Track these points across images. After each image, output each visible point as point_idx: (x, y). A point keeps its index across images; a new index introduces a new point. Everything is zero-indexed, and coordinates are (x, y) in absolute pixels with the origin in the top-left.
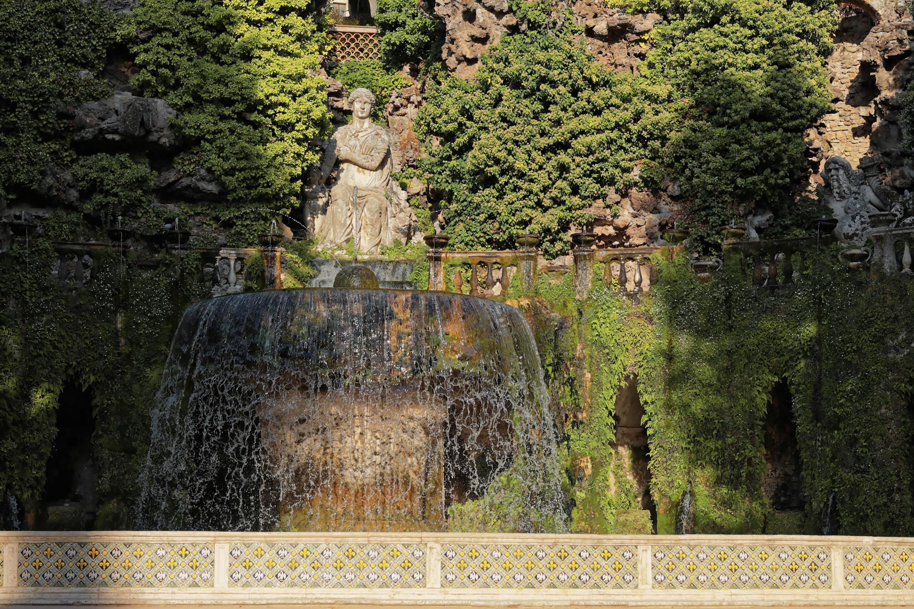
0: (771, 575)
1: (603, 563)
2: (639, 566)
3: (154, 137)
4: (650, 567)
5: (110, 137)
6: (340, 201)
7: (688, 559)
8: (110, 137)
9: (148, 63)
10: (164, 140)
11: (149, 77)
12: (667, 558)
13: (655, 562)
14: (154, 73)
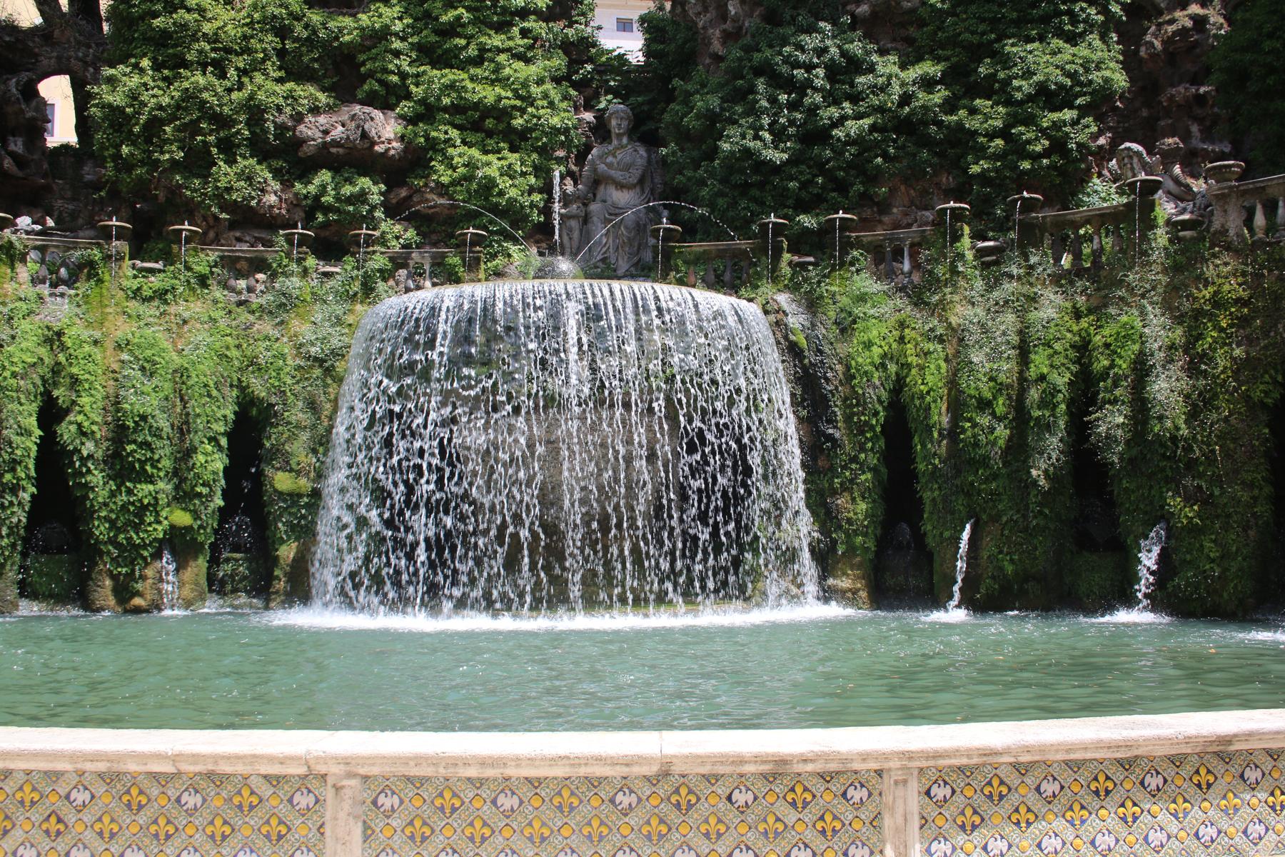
0: (1224, 825)
1: (791, 816)
2: (887, 822)
3: (379, 149)
4: (916, 822)
5: (334, 150)
6: (595, 219)
7: (1014, 799)
8: (334, 150)
9: (376, 72)
10: (392, 152)
11: (377, 87)
12: (959, 799)
13: (932, 811)
14: (380, 82)
